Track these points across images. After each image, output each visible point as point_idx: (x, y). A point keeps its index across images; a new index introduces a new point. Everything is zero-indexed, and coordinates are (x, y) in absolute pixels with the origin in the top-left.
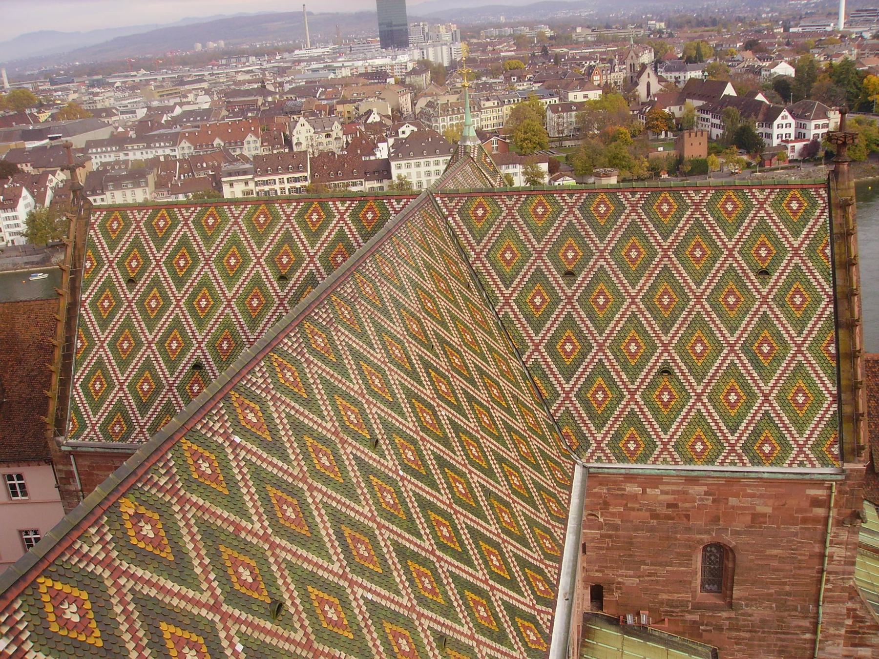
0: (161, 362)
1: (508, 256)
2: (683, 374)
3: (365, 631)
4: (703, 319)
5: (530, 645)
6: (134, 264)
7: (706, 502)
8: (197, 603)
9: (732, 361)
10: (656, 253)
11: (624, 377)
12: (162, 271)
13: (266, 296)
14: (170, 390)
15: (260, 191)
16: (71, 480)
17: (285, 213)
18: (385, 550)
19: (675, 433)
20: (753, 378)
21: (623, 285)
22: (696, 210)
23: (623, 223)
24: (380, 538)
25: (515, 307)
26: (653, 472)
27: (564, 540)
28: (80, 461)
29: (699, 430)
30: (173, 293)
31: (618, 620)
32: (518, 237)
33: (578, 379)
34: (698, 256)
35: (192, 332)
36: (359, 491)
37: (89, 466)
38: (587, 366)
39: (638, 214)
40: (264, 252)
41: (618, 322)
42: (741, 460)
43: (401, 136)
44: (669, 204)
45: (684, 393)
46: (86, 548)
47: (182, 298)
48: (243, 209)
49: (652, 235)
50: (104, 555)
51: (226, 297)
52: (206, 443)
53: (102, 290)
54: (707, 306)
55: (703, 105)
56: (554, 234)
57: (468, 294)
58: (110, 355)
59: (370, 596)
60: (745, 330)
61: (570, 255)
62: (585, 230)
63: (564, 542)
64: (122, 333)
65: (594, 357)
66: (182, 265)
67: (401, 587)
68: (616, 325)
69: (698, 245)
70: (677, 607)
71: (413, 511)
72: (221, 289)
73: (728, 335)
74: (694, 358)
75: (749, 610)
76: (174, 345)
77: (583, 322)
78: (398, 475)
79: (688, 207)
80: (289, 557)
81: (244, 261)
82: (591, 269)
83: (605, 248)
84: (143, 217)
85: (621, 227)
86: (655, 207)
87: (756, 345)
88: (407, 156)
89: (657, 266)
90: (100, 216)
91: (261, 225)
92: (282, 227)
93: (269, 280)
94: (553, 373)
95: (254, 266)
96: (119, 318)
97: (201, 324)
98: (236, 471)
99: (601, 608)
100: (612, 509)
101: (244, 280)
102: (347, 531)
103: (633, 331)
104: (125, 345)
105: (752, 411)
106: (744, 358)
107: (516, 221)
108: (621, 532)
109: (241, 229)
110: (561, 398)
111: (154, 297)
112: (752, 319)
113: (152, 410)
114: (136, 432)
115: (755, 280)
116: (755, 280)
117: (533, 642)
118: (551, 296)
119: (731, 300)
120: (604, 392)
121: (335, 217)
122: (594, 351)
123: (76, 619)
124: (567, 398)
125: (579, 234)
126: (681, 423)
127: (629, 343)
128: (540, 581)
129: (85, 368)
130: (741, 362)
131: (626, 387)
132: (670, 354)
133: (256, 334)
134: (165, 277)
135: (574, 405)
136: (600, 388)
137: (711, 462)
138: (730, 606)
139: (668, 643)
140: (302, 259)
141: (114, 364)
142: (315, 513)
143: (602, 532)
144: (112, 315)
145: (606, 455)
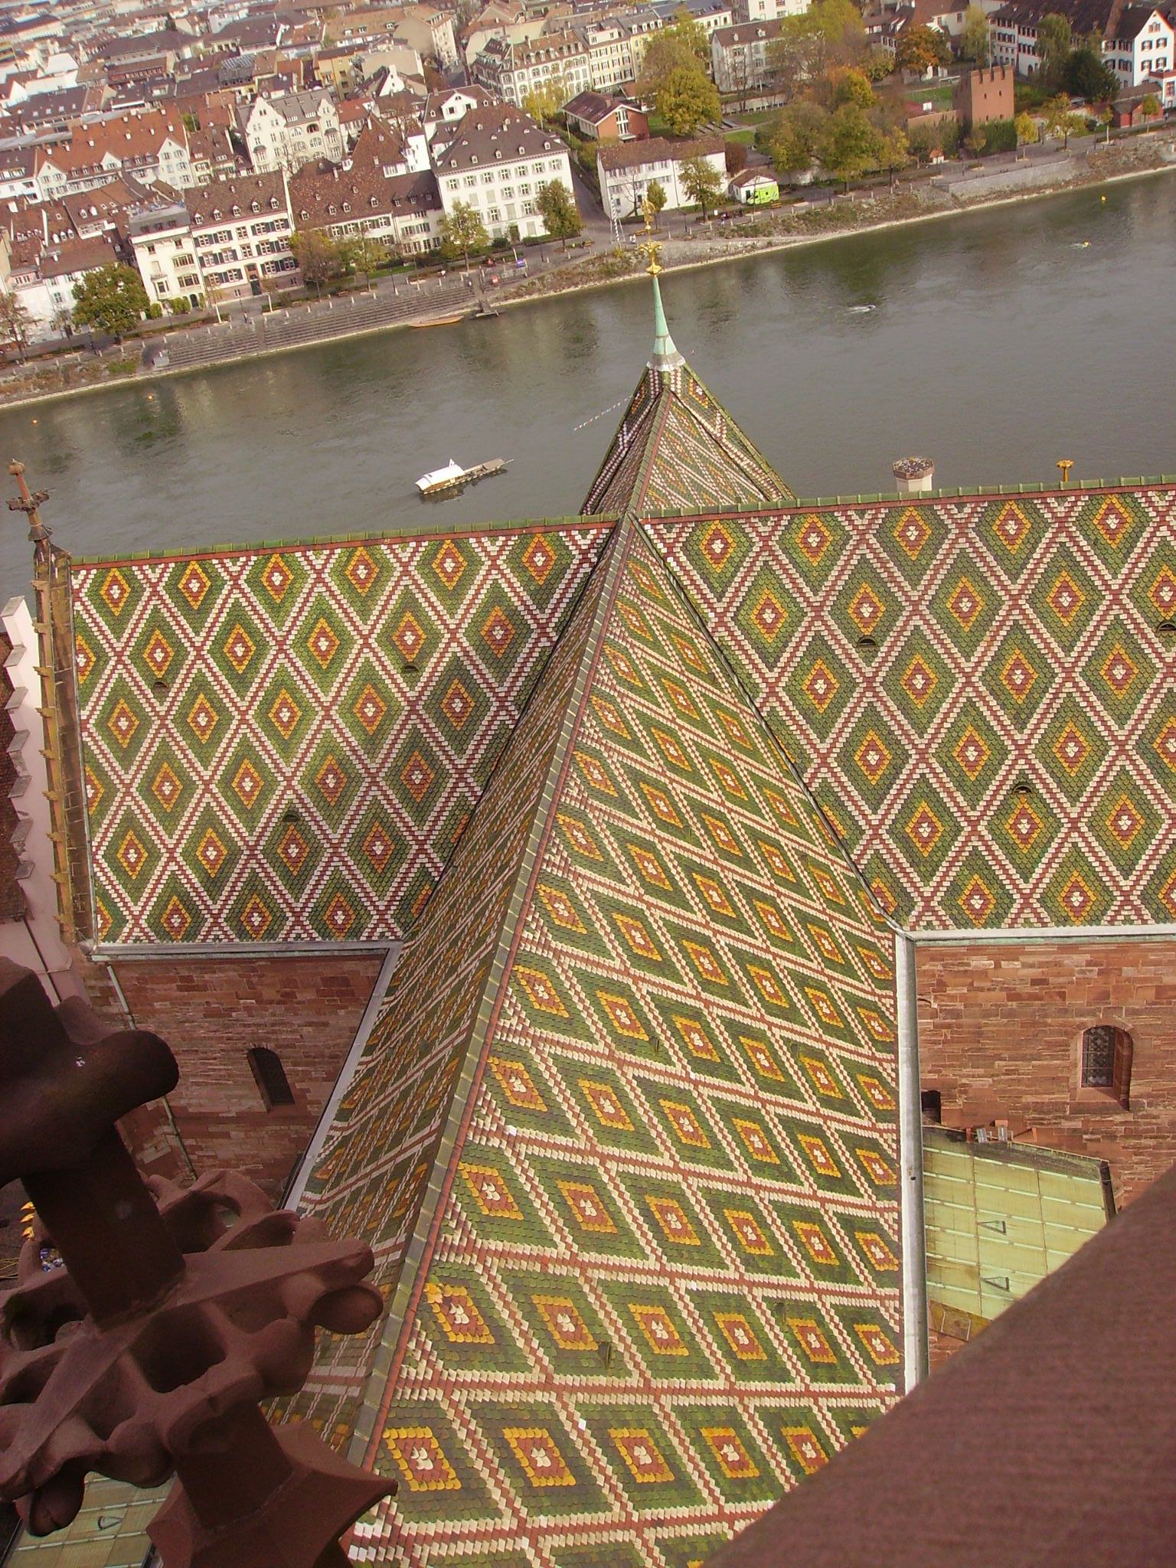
0: (231, 812)
1: (768, 616)
2: (1050, 791)
3: (698, 1338)
4: (1076, 705)
5: (877, 1268)
6: (159, 655)
7: (1088, 975)
8: (529, 1387)
9: (1123, 767)
10: (1001, 603)
11: (960, 799)
12: (208, 666)
13: (388, 698)
14: (252, 856)
15: (206, 254)
16: (111, 999)
17: (399, 560)
18: (697, 1208)
19: (1040, 880)
20: (1154, 792)
21: (951, 656)
22: (1060, 530)
23: (947, 556)
24: (688, 1193)
25: (786, 699)
26: (1010, 941)
27: (896, 1080)
28: (122, 972)
29: (1075, 874)
30: (232, 700)
31: (964, 1134)
32: (782, 586)
33: (891, 806)
34: (1066, 604)
35: (274, 761)
36: (654, 1134)
37: (138, 979)
38: (903, 786)
39: (969, 541)
40: (374, 627)
41: (946, 715)
42: (1140, 916)
44: (1018, 522)
45: (1051, 819)
46: (413, 1371)
47: (249, 708)
48: (329, 557)
49: (993, 573)
50: (431, 1372)
51: (321, 704)
52: (485, 1157)
53: (113, 701)
54: (1083, 684)
55: (1003, 9)
56: (838, 578)
57: (713, 693)
58: (145, 807)
59: (693, 1285)
60: (1141, 718)
61: (866, 611)
62: (887, 569)
63: (897, 1084)
64: (158, 770)
65: (912, 772)
66: (240, 654)
67: (723, 1254)
68: (944, 720)
69: (1065, 587)
70: (1049, 1112)
71: (716, 1130)
72: (311, 691)
73: (1115, 727)
74: (1065, 765)
75: (1153, 1111)
76: (248, 785)
77: (894, 718)
78: (690, 1081)
79: (1047, 525)
80: (602, 1275)
81: (343, 644)
82: (900, 633)
83: (921, 598)
84: (162, 576)
85: (943, 562)
86: (995, 528)
87: (1159, 740)
88: (466, 164)
89: (1002, 623)
90: (86, 577)
91: (362, 583)
92: (397, 583)
93: (388, 673)
94: (851, 798)
95: (361, 651)
97: (286, 749)
98: (522, 1180)
99: (938, 1120)
100: (950, 991)
101: (348, 675)
102: (652, 1201)
103: (970, 728)
104: (167, 789)
105: (1154, 842)
106: (1140, 762)
107: (776, 558)
108: (964, 1020)
109: (329, 589)
110: (866, 837)
111: (202, 709)
112: (1150, 701)
113: (227, 888)
114: (207, 924)
115: (1155, 640)
116: (1155, 640)
117: (880, 1262)
118: (840, 679)
119: (1119, 672)
120: (931, 824)
121: (483, 564)
122: (912, 761)
123: (429, 1466)
124: (876, 835)
125: (877, 576)
126: (1049, 865)
127: (966, 747)
128: (875, 1161)
129: (107, 830)
130: (1136, 767)
131: (964, 814)
132: (1028, 762)
133: (378, 761)
134: (214, 674)
135: (886, 846)
136: (924, 818)
137: (1095, 920)
138: (1126, 1105)
139: (1037, 1161)
140: (440, 637)
141: (153, 820)
142: (615, 1194)
143: (937, 1020)
144: (135, 742)
145: (939, 918)
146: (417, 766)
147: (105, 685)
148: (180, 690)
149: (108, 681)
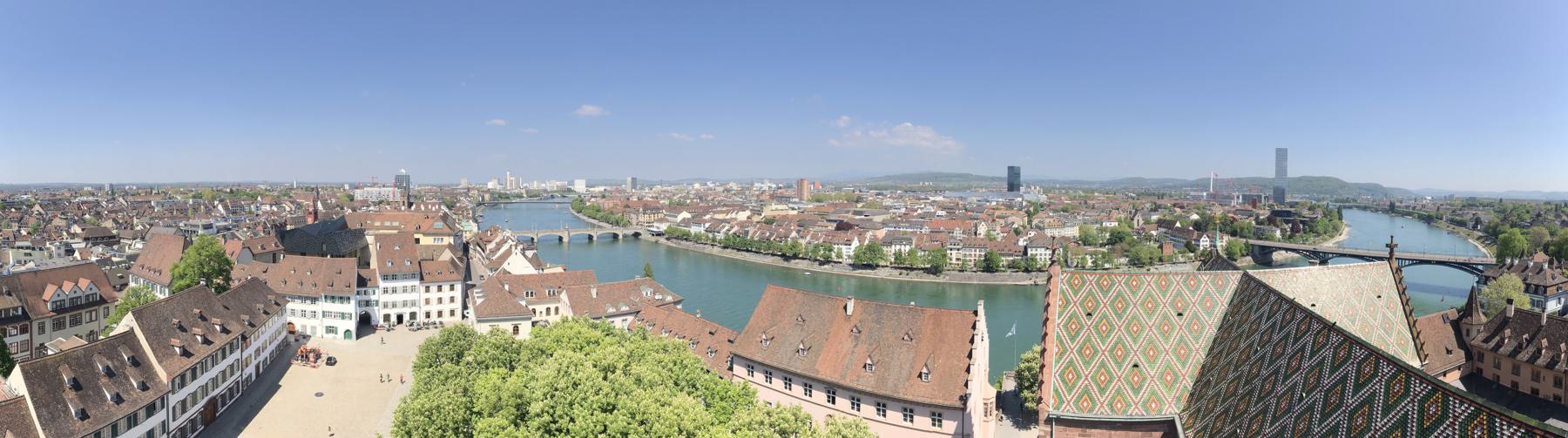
6: (1090, 305)
81: (1156, 306)
104: (1088, 352)
111: (1104, 324)
144: (1077, 334)
146: (1182, 348)
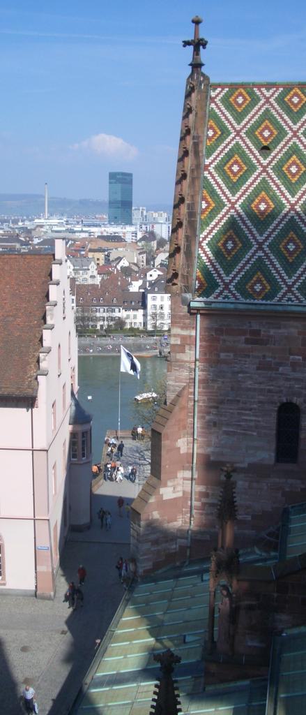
43: (149, 278)
53: (229, 156)
84: (273, 94)
90: (221, 92)
96: (252, 182)
111: (294, 163)
129: (213, 228)
144: (243, 179)
147: (225, 147)
148: (279, 152)
149: (228, 145)
